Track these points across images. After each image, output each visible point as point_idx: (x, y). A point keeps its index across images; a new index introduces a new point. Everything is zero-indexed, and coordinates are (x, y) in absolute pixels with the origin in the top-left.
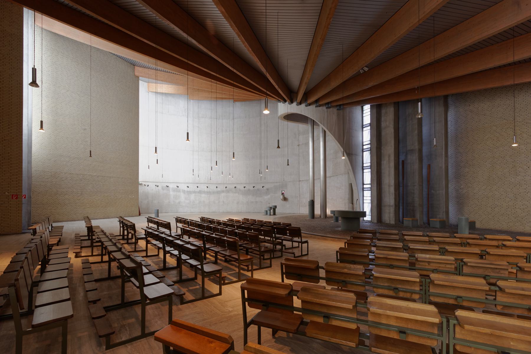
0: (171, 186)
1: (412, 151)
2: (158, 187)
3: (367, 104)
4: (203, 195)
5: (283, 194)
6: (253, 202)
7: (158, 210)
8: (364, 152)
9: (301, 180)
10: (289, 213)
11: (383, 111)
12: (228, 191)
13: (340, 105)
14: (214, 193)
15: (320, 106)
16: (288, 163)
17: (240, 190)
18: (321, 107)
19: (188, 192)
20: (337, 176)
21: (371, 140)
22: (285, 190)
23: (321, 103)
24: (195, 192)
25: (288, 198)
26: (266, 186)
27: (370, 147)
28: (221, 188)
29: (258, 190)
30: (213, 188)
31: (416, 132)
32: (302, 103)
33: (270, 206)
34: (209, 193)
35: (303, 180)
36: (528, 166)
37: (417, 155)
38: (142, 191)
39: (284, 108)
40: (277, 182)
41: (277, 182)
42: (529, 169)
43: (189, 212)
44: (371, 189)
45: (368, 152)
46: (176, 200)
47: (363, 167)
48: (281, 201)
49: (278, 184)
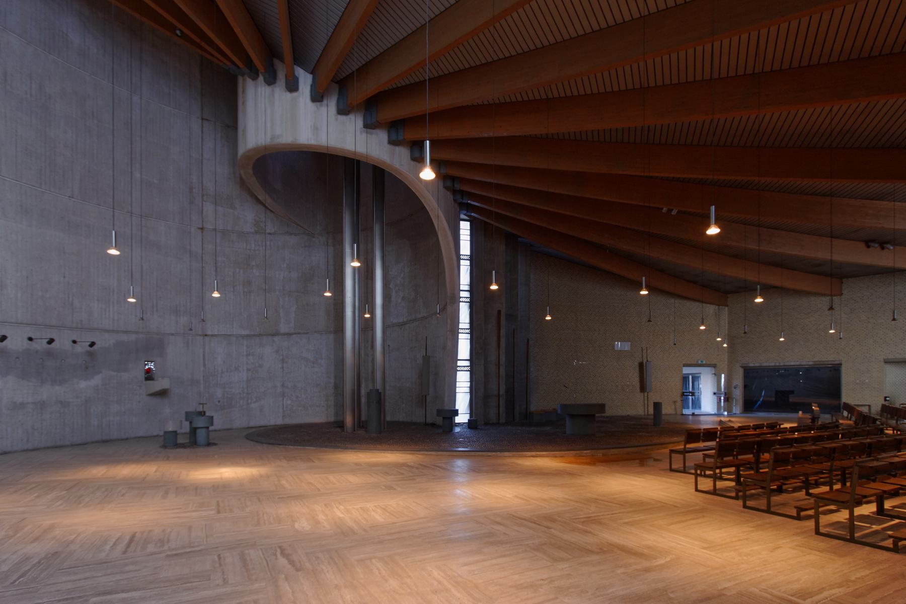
6: (22, 405)
9: (209, 333)
20: (307, 333)
35: (216, 333)
40: (126, 332)
41: (126, 332)
49: (133, 337)
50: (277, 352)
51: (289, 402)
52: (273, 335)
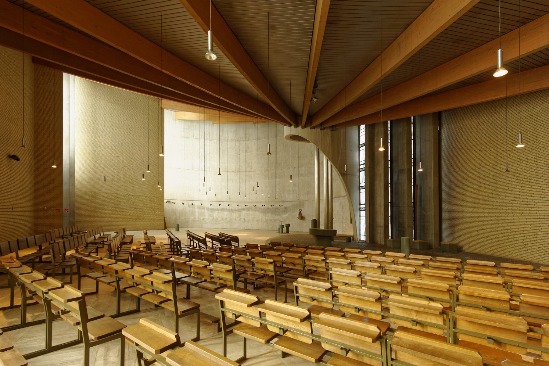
0: (196, 204)
1: (402, 171)
2: (175, 204)
3: (363, 124)
4: (225, 213)
5: (300, 212)
6: (272, 220)
7: (178, 225)
8: (361, 172)
10: (306, 231)
11: (376, 131)
12: (248, 209)
13: (332, 127)
14: (235, 210)
15: (314, 128)
16: (258, 185)
17: (259, 208)
18: (316, 129)
19: (211, 209)
21: (366, 160)
22: (302, 209)
23: (325, 126)
24: (218, 210)
25: (305, 216)
26: (285, 205)
27: (364, 167)
28: (242, 206)
29: (277, 208)
30: (234, 206)
31: (405, 152)
32: (307, 127)
33: (282, 225)
34: (231, 211)
36: (508, 187)
37: (406, 175)
38: (170, 209)
39: (288, 130)
40: (294, 201)
41: (294, 201)
42: (508, 190)
43: (213, 228)
44: (365, 209)
45: (363, 171)
46: (201, 216)
47: (360, 186)
48: (298, 219)
49: (296, 203)
50: (340, 204)
51: (345, 225)
52: (339, 197)
